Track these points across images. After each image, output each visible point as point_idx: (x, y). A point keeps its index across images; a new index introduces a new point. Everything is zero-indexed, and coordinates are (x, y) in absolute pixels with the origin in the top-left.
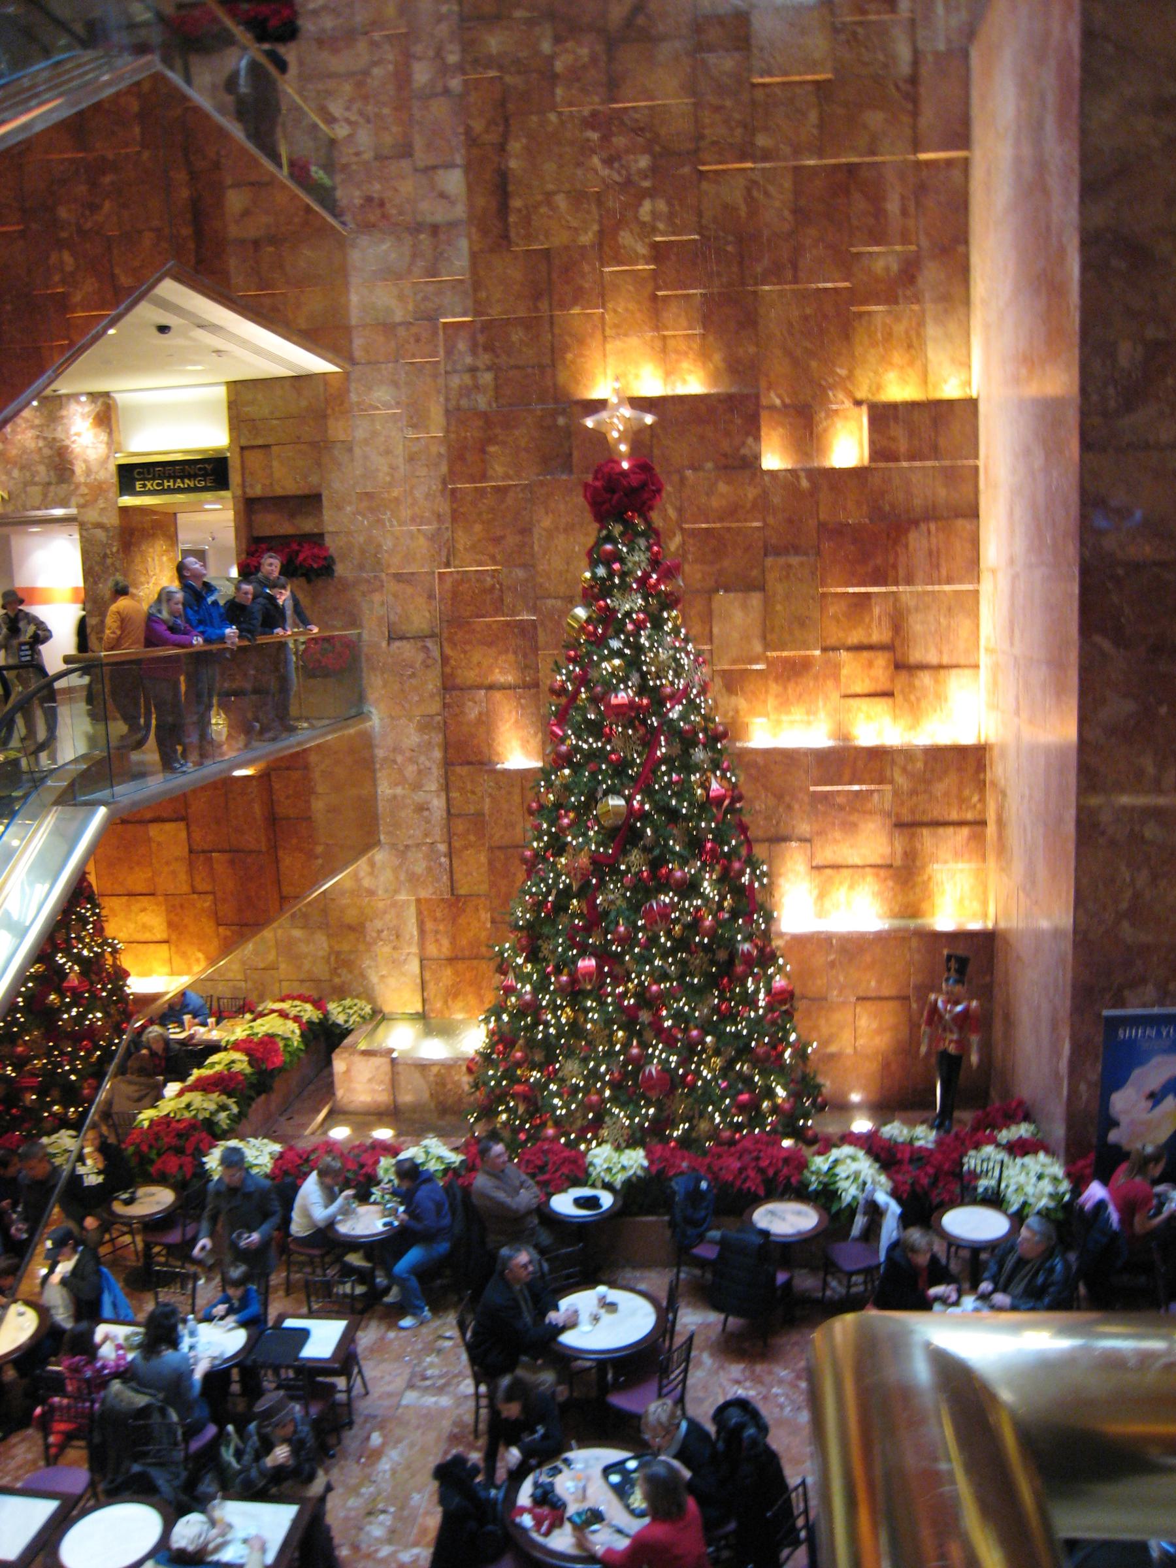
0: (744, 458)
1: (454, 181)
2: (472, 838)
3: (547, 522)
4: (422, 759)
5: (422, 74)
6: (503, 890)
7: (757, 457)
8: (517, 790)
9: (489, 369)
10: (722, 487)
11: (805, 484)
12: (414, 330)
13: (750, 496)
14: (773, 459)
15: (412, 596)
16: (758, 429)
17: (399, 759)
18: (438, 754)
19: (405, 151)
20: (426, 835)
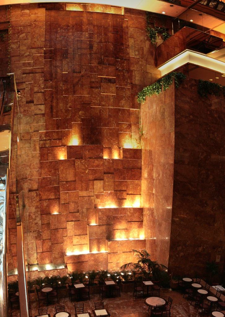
0: (100, 156)
1: (42, 107)
2: (46, 228)
3: (62, 168)
4: (36, 214)
5: (36, 89)
6: (54, 238)
7: (103, 156)
8: (56, 218)
9: (48, 140)
10: (96, 162)
11: (111, 162)
12: (34, 133)
13: (101, 163)
14: (106, 157)
15: (33, 183)
16: (103, 152)
17: (31, 214)
18: (39, 213)
19: (32, 102)
20: (37, 229)
